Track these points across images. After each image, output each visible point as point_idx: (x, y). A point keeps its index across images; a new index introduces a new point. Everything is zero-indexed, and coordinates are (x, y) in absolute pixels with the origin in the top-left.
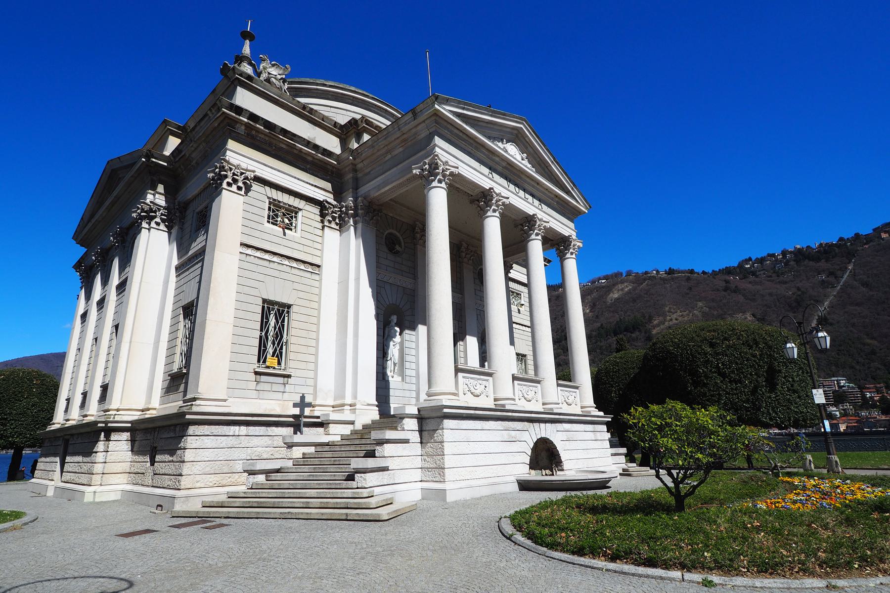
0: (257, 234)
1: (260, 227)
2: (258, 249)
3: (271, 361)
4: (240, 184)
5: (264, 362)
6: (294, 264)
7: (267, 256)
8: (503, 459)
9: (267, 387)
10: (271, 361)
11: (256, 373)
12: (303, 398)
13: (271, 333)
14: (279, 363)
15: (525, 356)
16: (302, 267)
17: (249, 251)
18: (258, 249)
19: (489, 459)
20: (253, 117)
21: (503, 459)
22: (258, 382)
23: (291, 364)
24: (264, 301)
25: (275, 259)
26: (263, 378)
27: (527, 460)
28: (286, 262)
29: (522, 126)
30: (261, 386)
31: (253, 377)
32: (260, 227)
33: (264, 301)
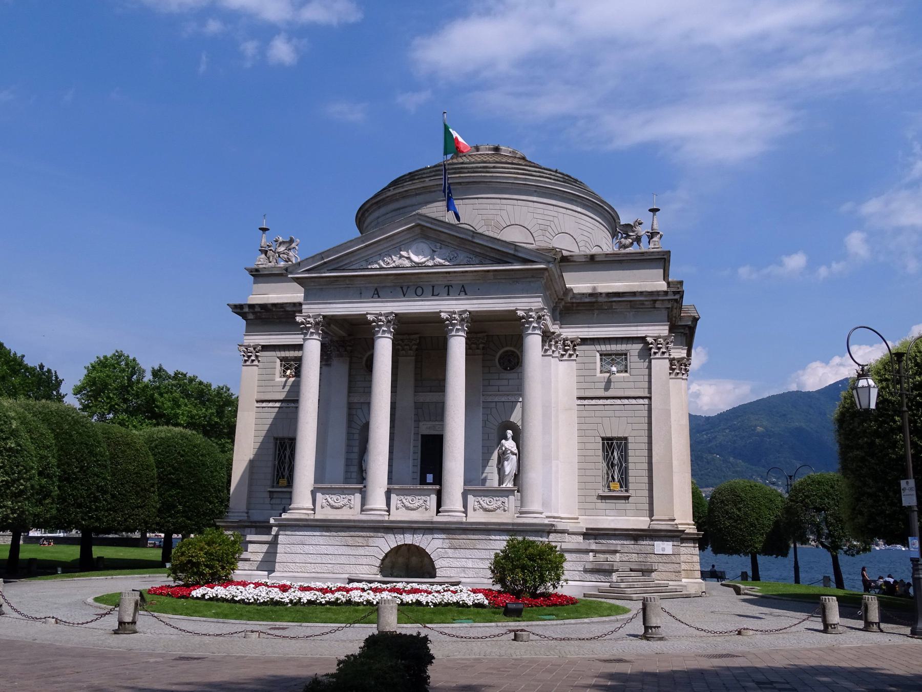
0: (270, 389)
1: (272, 383)
4: (253, 358)
5: (278, 483)
8: (343, 560)
9: (278, 501)
15: (626, 439)
17: (264, 405)
19: (325, 559)
20: (252, 306)
21: (343, 560)
22: (271, 498)
26: (275, 495)
27: (378, 563)
29: (419, 222)
30: (274, 501)
31: (267, 495)
32: (272, 383)
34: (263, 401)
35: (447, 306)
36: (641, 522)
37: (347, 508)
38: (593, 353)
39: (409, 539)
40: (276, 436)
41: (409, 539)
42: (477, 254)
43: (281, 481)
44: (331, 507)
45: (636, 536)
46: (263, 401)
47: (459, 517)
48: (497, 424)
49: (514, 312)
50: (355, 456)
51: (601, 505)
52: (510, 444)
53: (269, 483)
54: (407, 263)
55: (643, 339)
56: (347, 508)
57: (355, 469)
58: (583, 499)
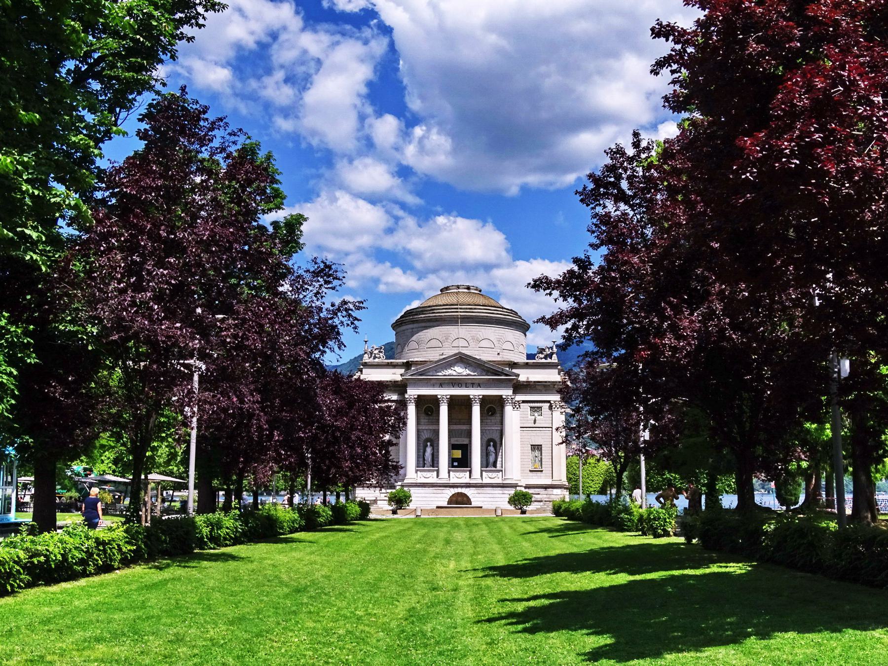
35: (475, 393)
36: (548, 482)
37: (431, 477)
38: (527, 406)
39: (460, 490)
41: (460, 490)
42: (484, 370)
44: (421, 478)
45: (546, 487)
47: (480, 481)
48: (494, 444)
49: (501, 396)
50: (421, 454)
51: (531, 474)
52: (492, 449)
54: (454, 373)
55: (549, 402)
56: (431, 477)
57: (421, 459)
58: (523, 471)
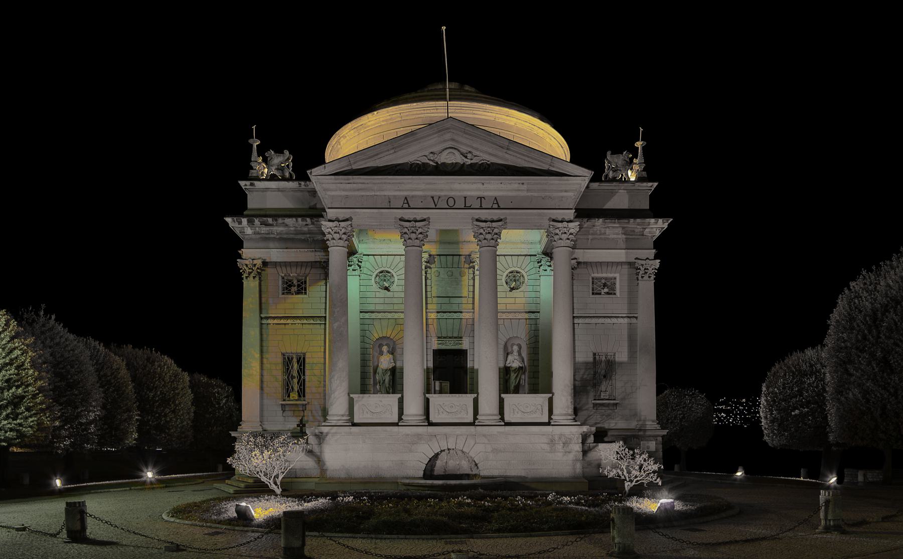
2: (274, 318)
3: (294, 395)
5: (289, 396)
6: (305, 321)
7: (282, 321)
10: (294, 395)
11: (282, 405)
12: (301, 421)
13: (295, 374)
14: (299, 396)
16: (312, 322)
17: (270, 321)
18: (274, 318)
22: (284, 411)
23: (307, 396)
24: (283, 355)
25: (289, 321)
28: (298, 321)
30: (286, 413)
33: (283, 355)
34: (267, 318)
40: (284, 351)
43: (291, 395)
46: (267, 318)
53: (280, 396)
